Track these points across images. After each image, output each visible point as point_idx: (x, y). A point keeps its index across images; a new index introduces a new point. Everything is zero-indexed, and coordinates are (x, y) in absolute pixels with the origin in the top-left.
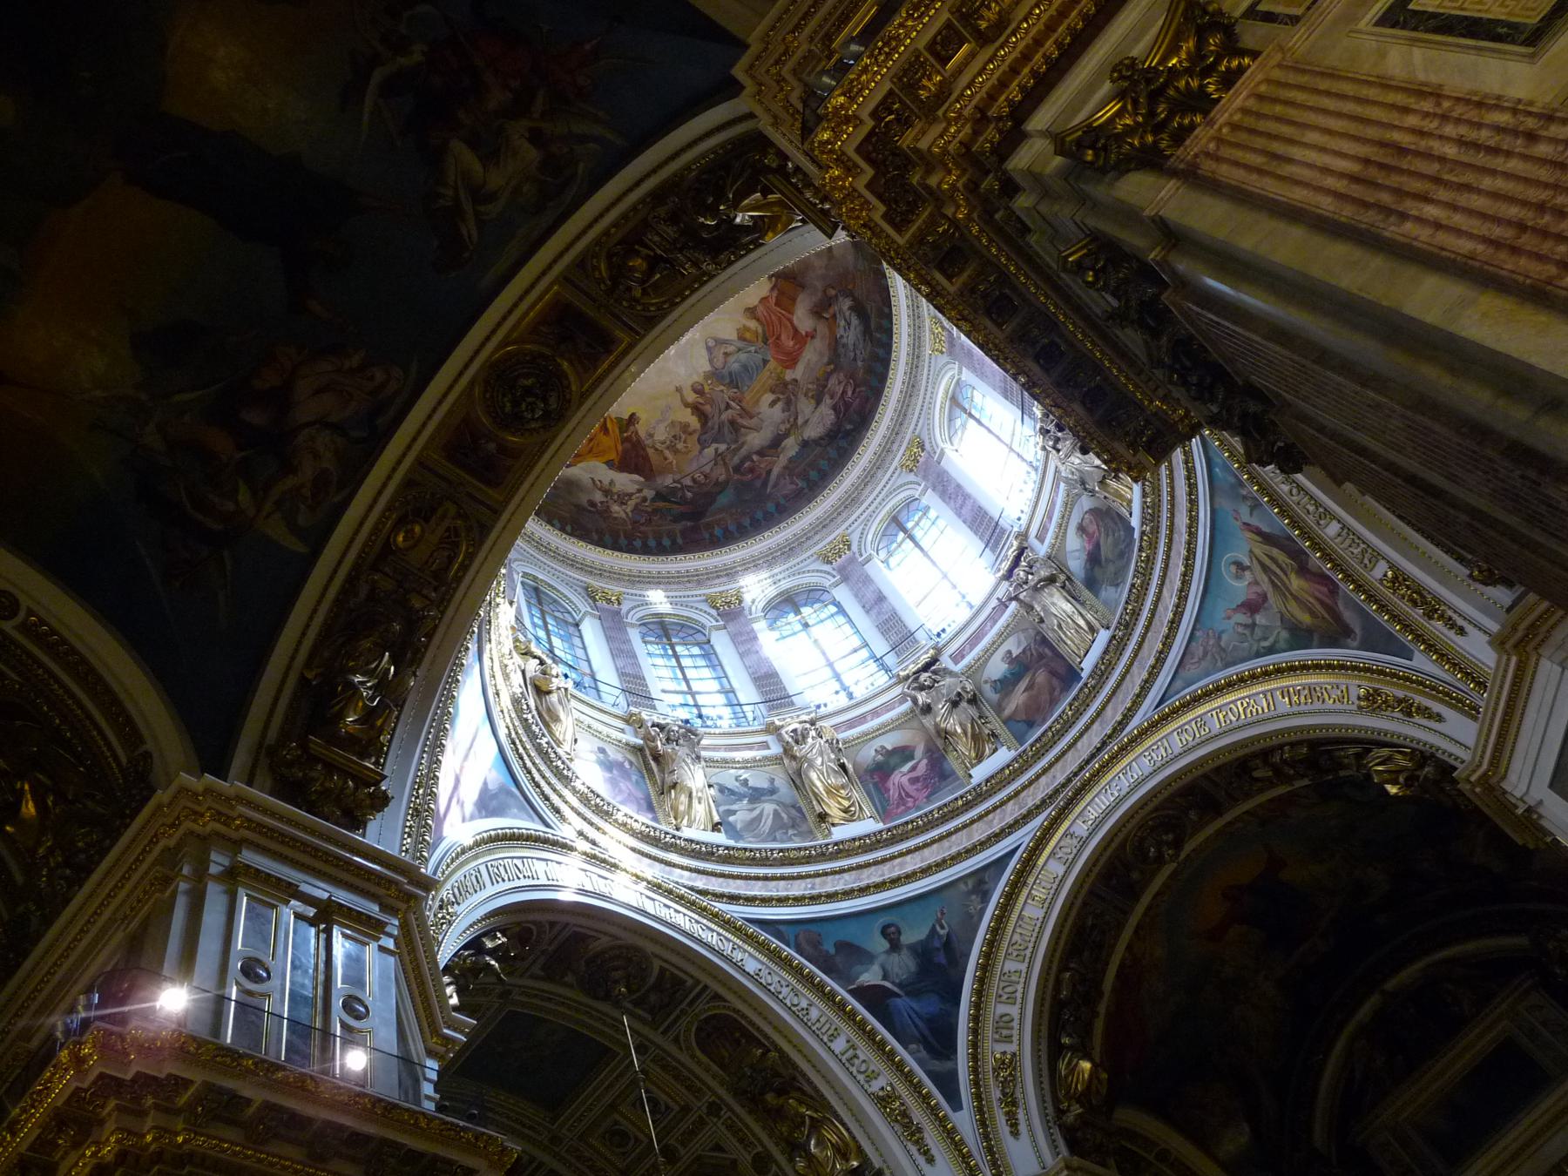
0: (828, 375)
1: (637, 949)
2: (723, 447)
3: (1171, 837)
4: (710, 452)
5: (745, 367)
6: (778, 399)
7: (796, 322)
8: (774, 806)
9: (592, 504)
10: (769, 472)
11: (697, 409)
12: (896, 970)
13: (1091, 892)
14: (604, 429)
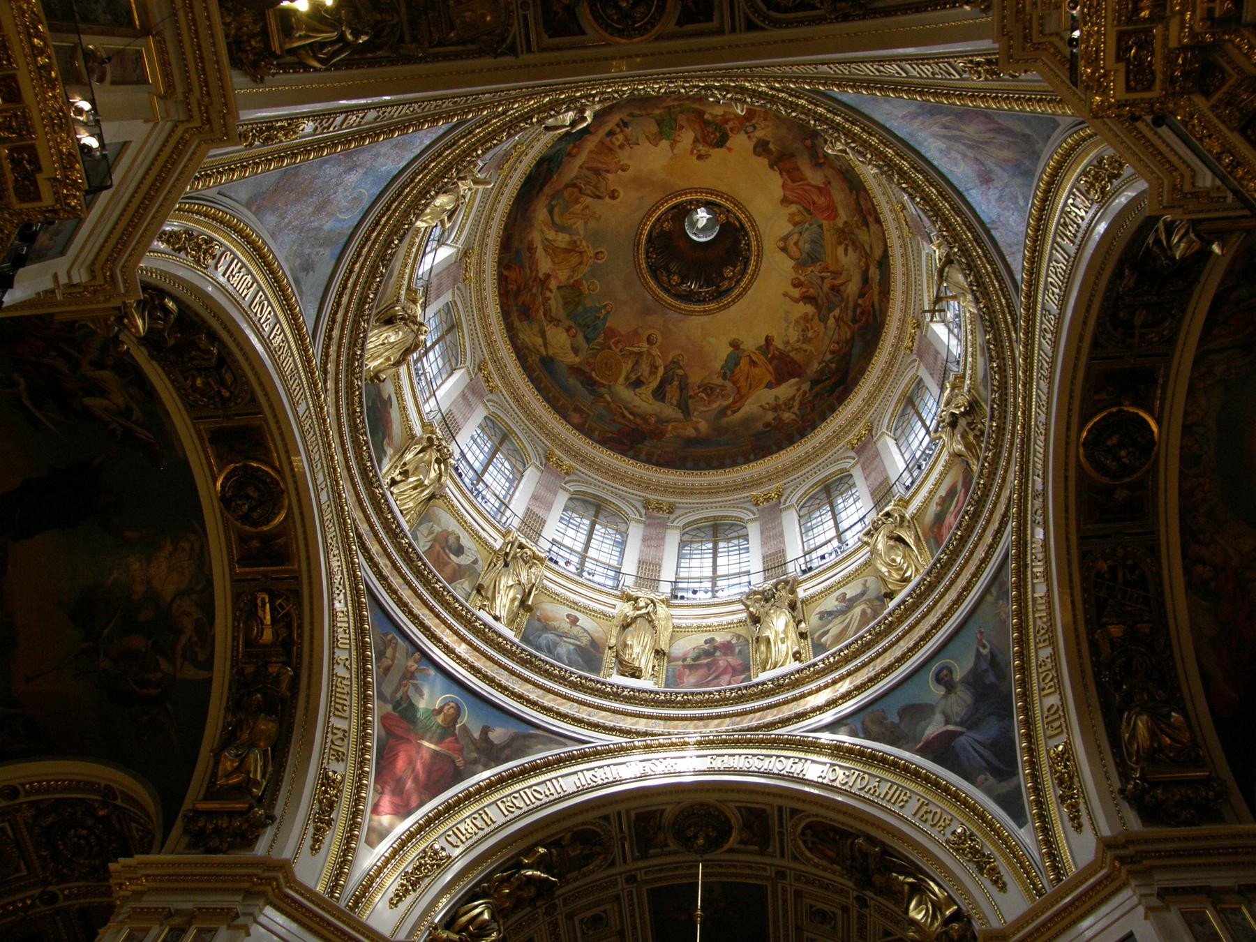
0: (857, 198)
1: (702, 804)
2: (837, 312)
3: (1115, 440)
4: (831, 322)
5: (813, 242)
6: (847, 246)
7: (814, 183)
8: (863, 606)
9: (767, 425)
10: (873, 306)
11: (806, 299)
12: (956, 709)
13: (1082, 539)
14: (753, 363)
